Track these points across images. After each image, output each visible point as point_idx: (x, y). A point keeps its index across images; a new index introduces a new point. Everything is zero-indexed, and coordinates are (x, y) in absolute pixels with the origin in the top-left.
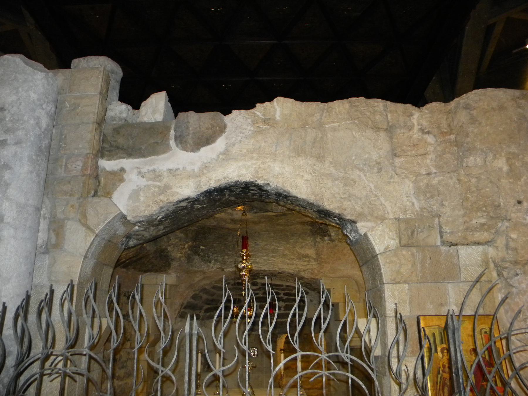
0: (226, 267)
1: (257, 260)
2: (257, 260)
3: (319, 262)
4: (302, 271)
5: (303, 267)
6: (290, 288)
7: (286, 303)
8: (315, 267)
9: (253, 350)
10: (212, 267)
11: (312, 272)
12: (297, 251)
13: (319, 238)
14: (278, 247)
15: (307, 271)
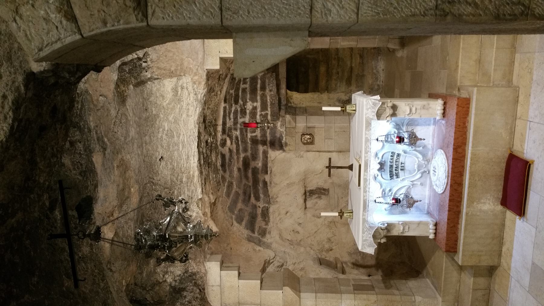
0: (195, 197)
1: (184, 157)
2: (184, 157)
3: (182, 74)
4: (197, 97)
5: (192, 95)
6: (228, 97)
7: (248, 100)
8: (190, 79)
9: (304, 138)
10: (197, 213)
11: (197, 83)
12: (169, 104)
13: (147, 74)
14: (164, 130)
15: (196, 90)
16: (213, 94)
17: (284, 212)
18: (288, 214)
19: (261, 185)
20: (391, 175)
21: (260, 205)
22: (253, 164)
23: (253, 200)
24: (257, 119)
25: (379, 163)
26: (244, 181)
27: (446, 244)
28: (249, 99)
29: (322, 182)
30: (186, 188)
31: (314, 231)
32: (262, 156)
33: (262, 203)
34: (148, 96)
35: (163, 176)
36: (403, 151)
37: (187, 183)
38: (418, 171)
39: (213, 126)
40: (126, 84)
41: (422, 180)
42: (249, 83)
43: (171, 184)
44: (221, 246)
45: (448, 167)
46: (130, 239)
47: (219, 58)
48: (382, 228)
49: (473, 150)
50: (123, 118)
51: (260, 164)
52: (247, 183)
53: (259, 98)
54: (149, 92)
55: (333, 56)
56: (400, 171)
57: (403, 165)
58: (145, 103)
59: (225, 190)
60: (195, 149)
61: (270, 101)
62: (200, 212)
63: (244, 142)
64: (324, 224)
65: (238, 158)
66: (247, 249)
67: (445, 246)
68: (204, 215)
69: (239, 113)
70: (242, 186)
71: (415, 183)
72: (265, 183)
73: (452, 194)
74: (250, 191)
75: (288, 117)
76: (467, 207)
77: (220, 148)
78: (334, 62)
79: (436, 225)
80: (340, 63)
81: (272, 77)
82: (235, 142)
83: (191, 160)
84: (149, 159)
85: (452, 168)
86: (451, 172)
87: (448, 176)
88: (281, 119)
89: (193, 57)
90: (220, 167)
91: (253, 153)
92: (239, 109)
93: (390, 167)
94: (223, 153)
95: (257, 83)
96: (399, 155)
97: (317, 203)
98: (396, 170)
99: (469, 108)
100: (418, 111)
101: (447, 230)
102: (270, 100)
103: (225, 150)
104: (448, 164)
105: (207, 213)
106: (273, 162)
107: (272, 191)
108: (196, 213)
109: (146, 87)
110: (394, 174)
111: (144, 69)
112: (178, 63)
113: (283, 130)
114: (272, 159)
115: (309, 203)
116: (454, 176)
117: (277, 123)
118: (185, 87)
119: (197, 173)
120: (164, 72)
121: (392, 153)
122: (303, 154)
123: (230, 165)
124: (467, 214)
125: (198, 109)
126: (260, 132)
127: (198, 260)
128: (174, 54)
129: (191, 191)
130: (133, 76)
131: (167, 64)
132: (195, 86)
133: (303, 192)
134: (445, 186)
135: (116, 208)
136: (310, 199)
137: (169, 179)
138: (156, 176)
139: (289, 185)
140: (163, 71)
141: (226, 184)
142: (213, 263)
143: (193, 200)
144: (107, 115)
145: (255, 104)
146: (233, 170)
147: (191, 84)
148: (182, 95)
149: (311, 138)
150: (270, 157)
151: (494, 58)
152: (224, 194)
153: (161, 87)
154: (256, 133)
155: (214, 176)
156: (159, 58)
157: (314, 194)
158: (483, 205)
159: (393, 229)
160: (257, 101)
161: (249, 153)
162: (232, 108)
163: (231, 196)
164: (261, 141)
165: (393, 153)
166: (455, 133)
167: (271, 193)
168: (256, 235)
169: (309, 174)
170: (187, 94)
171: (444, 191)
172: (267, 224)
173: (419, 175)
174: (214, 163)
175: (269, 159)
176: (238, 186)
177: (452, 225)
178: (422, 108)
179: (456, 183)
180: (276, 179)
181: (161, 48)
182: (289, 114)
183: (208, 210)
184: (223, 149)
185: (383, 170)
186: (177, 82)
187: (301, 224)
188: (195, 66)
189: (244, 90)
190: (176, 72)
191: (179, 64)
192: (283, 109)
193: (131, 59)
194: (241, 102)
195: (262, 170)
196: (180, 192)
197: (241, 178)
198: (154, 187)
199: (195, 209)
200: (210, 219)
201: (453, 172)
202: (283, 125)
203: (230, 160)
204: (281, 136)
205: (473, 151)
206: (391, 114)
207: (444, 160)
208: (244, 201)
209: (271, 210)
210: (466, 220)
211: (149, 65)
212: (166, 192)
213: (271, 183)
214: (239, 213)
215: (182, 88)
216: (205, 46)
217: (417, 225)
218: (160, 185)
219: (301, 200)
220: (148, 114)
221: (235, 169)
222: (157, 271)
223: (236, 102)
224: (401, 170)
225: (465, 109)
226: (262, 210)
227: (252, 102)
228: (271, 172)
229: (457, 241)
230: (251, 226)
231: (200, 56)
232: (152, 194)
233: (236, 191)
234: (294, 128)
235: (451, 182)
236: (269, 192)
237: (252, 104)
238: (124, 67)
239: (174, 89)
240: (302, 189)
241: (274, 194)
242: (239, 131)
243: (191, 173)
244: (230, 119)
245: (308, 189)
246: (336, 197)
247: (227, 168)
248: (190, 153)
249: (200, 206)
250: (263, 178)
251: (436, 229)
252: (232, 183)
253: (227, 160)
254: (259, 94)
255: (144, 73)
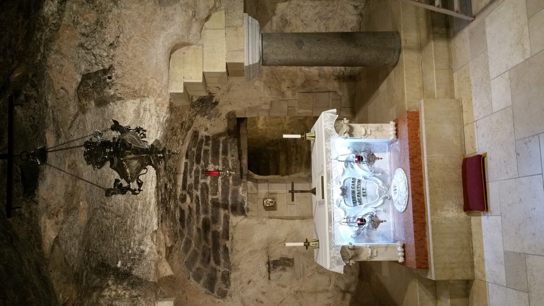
0: (150, 228)
3: (146, 95)
6: (189, 154)
7: (210, 162)
9: (266, 202)
10: (151, 248)
11: (160, 105)
15: (159, 112)
16: (175, 137)
17: (246, 280)
18: (251, 284)
19: (221, 250)
20: (354, 201)
21: (220, 269)
22: (213, 228)
23: (212, 263)
24: (219, 182)
25: (341, 188)
26: (203, 243)
27: (417, 260)
28: (211, 161)
29: (286, 252)
30: (140, 218)
31: (279, 301)
32: (224, 220)
33: (223, 267)
34: (108, 117)
35: (116, 201)
36: (363, 177)
37: (142, 210)
38: (380, 196)
39: (173, 173)
40: (88, 98)
41: (384, 206)
42: (211, 145)
43: (125, 212)
44: (175, 293)
45: (407, 179)
46: (72, 258)
47: (183, 83)
48: (350, 248)
49: (428, 157)
50: (81, 124)
51: (221, 229)
52: (206, 245)
53: (220, 161)
54: (110, 113)
55: (292, 144)
56: (362, 197)
57: (364, 191)
58: (105, 123)
59: (183, 245)
60: (154, 174)
61: (232, 166)
62: (154, 246)
63: (205, 202)
64: (289, 293)
65: (198, 218)
66: (205, 302)
67: (415, 261)
68: (159, 252)
69: (200, 173)
70: (201, 247)
71: (378, 209)
72: (226, 249)
73: (415, 205)
74: (210, 253)
75: (250, 183)
76: (431, 215)
77: (179, 203)
78: (293, 149)
79: (404, 247)
80: (299, 150)
81: (234, 142)
82: (195, 201)
83: (148, 185)
84: (102, 181)
85: (411, 178)
86: (411, 182)
87: (409, 188)
88: (242, 184)
89: (157, 78)
90: (178, 221)
91: (214, 216)
92: (200, 170)
93: (352, 193)
94: (182, 209)
95: (219, 146)
96: (359, 181)
97: (281, 275)
98: (358, 196)
99: (418, 120)
100: (373, 133)
101: (415, 243)
102: (232, 165)
103: (185, 206)
104: (407, 176)
105: (162, 253)
106: (235, 228)
107: (234, 258)
108: (150, 248)
109: (108, 108)
110: (357, 200)
111: (108, 84)
112: (142, 82)
113: (245, 195)
114: (234, 225)
115: (273, 275)
116: (414, 186)
117: (239, 188)
118: (148, 109)
119: (153, 201)
120: (128, 90)
121: (353, 179)
122: (265, 221)
123: (189, 223)
124: (432, 222)
125: (159, 132)
126: (222, 196)
127: (149, 298)
128: (139, 73)
129: (146, 220)
130: (95, 91)
131: (132, 82)
132: (158, 108)
133: (266, 260)
134: (407, 200)
135: (62, 210)
136: (273, 271)
137: (123, 205)
138: (108, 201)
139: (251, 253)
140: (128, 90)
141: (184, 240)
142: (166, 302)
143: (148, 232)
144: (66, 107)
145: (217, 167)
146: (192, 228)
147: (154, 106)
148: (144, 117)
149: (273, 201)
150: (232, 223)
151: (435, 78)
152: (181, 248)
153: (123, 108)
154: (218, 196)
155: (172, 224)
156: (124, 74)
157: (278, 266)
158: (446, 212)
159: (361, 254)
160: (219, 165)
161: (209, 216)
162: (193, 166)
163: (189, 254)
164: (223, 204)
165: (354, 179)
166: (409, 144)
167: (232, 260)
168: (216, 294)
169: (272, 243)
170: (149, 116)
171: (407, 205)
172: (228, 286)
173: (381, 202)
174: (172, 211)
175: (230, 225)
176: (197, 245)
177: (420, 238)
178: (376, 130)
179: (417, 193)
180: (238, 246)
181: (127, 65)
182: (251, 181)
183: (163, 250)
184: (182, 204)
185: (346, 196)
186: (140, 104)
187: (264, 293)
188: (159, 87)
189: (206, 151)
190: (140, 92)
191: (144, 83)
192: (245, 179)
193: (96, 70)
194: (202, 163)
195: (223, 235)
196: (134, 222)
197: (200, 239)
198: (105, 213)
199: (148, 243)
200: (164, 259)
201: (412, 182)
202: (245, 190)
203: (189, 218)
204: (243, 201)
205: (429, 158)
206: (348, 130)
207: (402, 175)
208: (203, 262)
209: (232, 276)
210: (433, 229)
211: (113, 81)
212: (117, 221)
213: (232, 250)
214: (197, 272)
215: (145, 110)
216: (170, 72)
217: (384, 249)
218: (112, 212)
219: (264, 269)
220: (107, 135)
221: (195, 231)
222: (100, 302)
223: (198, 162)
224: (363, 196)
225: (415, 122)
226: (222, 274)
227: (213, 164)
228: (232, 239)
229: (428, 256)
230: (210, 285)
231: (165, 79)
232: (102, 222)
233: (195, 250)
234: (256, 194)
235: (412, 192)
236: (230, 259)
237: (214, 167)
238: (89, 81)
239: (136, 111)
240: (265, 257)
241: (236, 262)
242: (199, 191)
243: (148, 199)
244: (191, 177)
245: (272, 259)
246: (301, 265)
247: (186, 225)
248: (148, 178)
249: (155, 240)
250: (224, 243)
251: (404, 252)
252: (191, 241)
253: (186, 217)
254: (221, 158)
255: (107, 90)
